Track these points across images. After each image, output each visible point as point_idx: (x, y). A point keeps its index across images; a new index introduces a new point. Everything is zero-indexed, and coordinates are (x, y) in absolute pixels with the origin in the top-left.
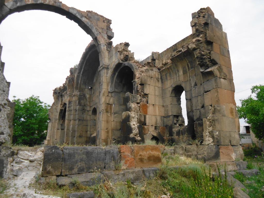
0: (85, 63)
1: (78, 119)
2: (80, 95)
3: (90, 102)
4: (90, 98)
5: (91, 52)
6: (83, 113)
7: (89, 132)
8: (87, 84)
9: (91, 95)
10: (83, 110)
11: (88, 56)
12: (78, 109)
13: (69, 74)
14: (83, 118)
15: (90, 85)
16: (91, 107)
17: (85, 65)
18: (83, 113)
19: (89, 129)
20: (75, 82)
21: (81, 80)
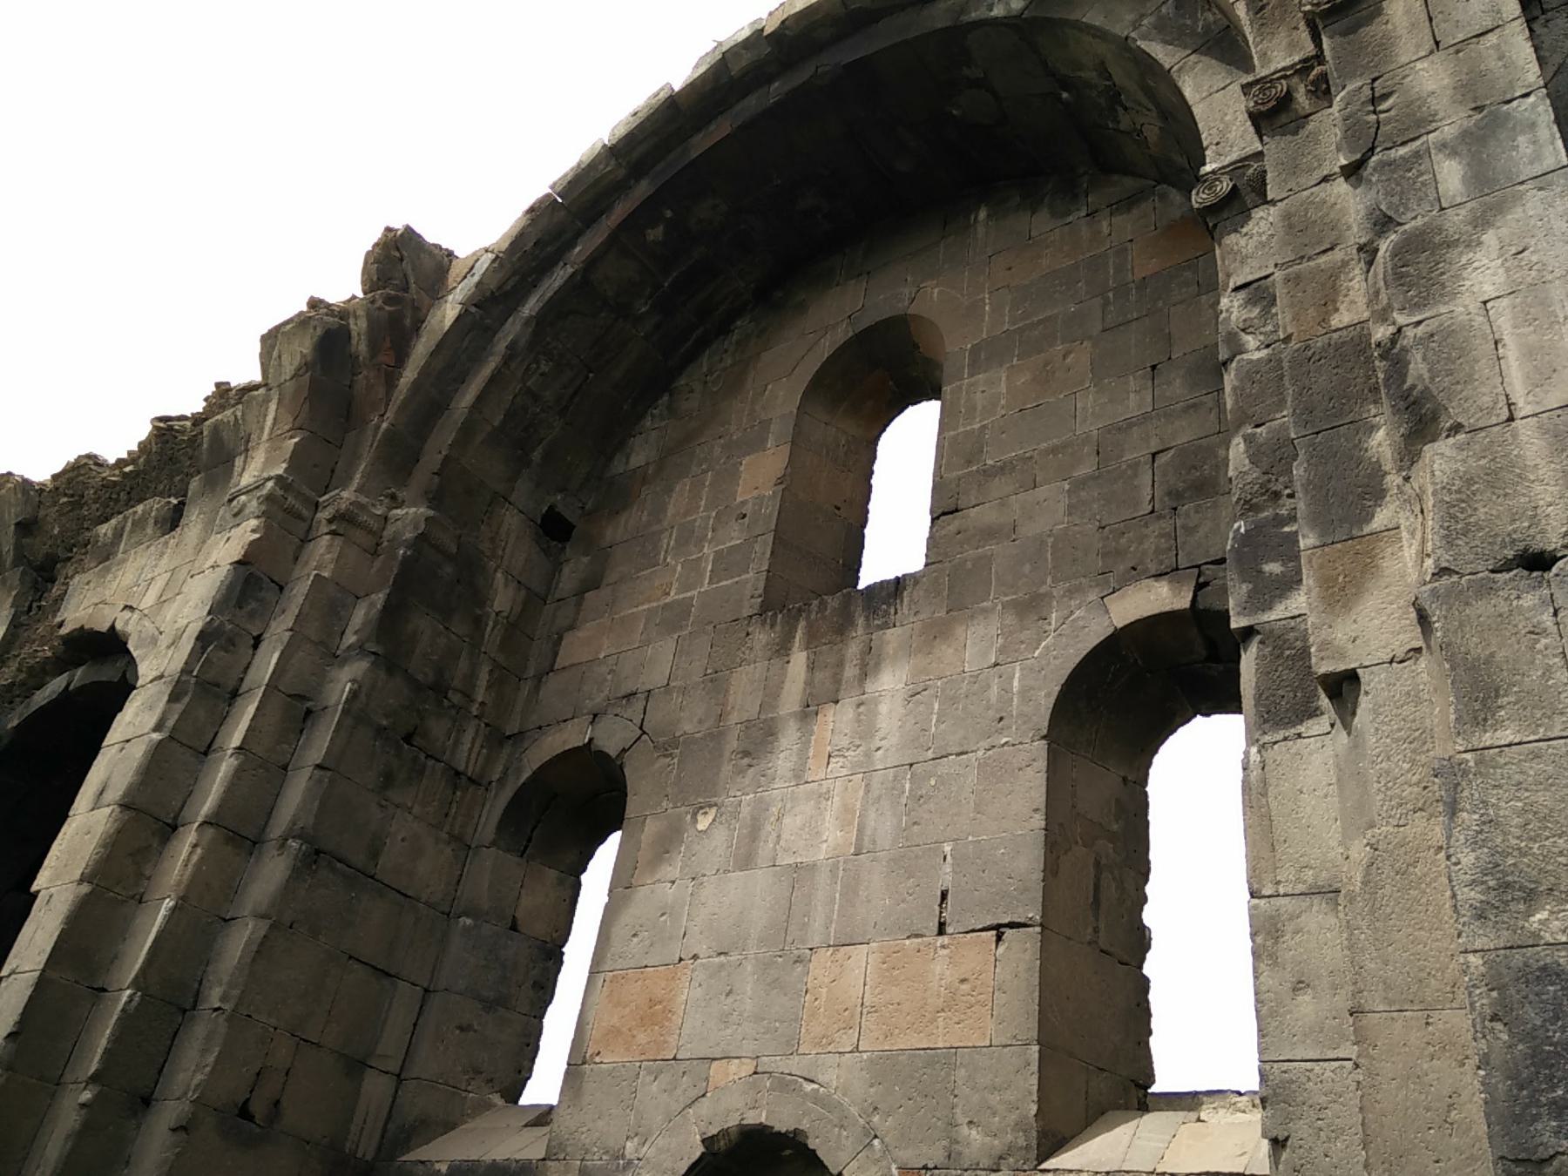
0: (621, 210)
1: (301, 836)
2: (422, 538)
3: (504, 678)
4: (517, 628)
5: (778, 89)
6: (388, 780)
7: (375, 1088)
8: (536, 456)
9: (535, 599)
10: (408, 739)
11: (721, 129)
12: (354, 695)
13: (343, 284)
14: (374, 854)
15: (562, 490)
16: (499, 739)
17: (624, 225)
18: (388, 780)
19: (390, 1045)
20: (409, 375)
21: (492, 380)
